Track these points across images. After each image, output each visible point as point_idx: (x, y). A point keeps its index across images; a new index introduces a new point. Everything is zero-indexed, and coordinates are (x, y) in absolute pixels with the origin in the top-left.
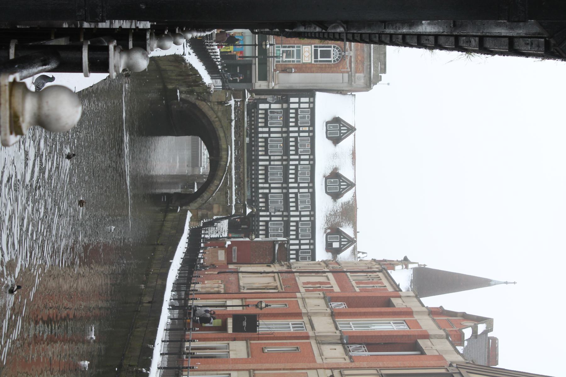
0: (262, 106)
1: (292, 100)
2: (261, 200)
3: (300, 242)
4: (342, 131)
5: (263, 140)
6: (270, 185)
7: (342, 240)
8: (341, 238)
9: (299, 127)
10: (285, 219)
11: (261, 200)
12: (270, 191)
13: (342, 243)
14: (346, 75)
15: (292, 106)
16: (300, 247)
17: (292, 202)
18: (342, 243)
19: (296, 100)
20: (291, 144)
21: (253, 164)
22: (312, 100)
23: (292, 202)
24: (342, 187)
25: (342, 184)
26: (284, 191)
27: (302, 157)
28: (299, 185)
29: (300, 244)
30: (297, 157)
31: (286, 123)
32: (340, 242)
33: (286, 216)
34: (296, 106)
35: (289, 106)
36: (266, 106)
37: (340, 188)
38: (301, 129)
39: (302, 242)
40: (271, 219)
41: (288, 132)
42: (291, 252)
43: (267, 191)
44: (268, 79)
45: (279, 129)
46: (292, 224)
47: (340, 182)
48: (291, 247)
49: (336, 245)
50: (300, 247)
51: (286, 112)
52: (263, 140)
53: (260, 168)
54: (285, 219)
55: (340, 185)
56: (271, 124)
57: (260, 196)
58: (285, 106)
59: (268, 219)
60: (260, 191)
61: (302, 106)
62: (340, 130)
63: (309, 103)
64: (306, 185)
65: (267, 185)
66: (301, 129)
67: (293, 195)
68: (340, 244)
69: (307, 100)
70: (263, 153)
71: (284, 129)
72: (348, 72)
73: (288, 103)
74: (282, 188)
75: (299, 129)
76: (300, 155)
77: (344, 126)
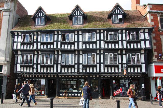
0: (19, 69)
1: (15, 48)
2: (88, 71)
3: (120, 41)
4: (41, 16)
5: (42, 69)
6: (76, 64)
7: (116, 13)
8: (115, 14)
9: (34, 42)
10: (102, 52)
11: (88, 71)
12: (81, 64)
13: (119, 13)
14: (5, 13)
15: (19, 47)
16: (125, 40)
17: (89, 46)
18: (119, 13)
19: (15, 44)
20: (45, 47)
21: (60, 76)
22: (16, 34)
23: (89, 46)
24: (79, 14)
25: (76, 14)
26: (81, 53)
27: (56, 39)
28: (76, 42)
29: (122, 40)
30: (55, 43)
31: (32, 52)
32: (118, 14)
33: (100, 52)
34: (19, 44)
35: (19, 50)
36: (19, 66)
37: (80, 15)
38: (35, 41)
39: (120, 39)
40: (103, 63)
41: (37, 50)
42: (129, 47)
43: (81, 66)
44: (1, 65)
45: (36, 57)
46: (106, 47)
47: (75, 16)
48: (125, 47)
49: (120, 17)
50: (125, 40)
51: (23, 51)
52: (42, 69)
53: (63, 71)
54: (102, 52)
55: (78, 15)
56: (31, 63)
57: (84, 71)
58: (19, 53)
59: (102, 65)
60: (81, 71)
61: (19, 40)
62: (40, 17)
63: (18, 35)
64: (76, 36)
65: (76, 66)
66: (35, 41)
67: (84, 45)
68: (120, 14)
69: (16, 37)
70: (52, 69)
71: (36, 53)
72: (3, 13)
73: (16, 51)
74: (79, 55)
75: (35, 42)
76: (54, 41)
77: (38, 15)
